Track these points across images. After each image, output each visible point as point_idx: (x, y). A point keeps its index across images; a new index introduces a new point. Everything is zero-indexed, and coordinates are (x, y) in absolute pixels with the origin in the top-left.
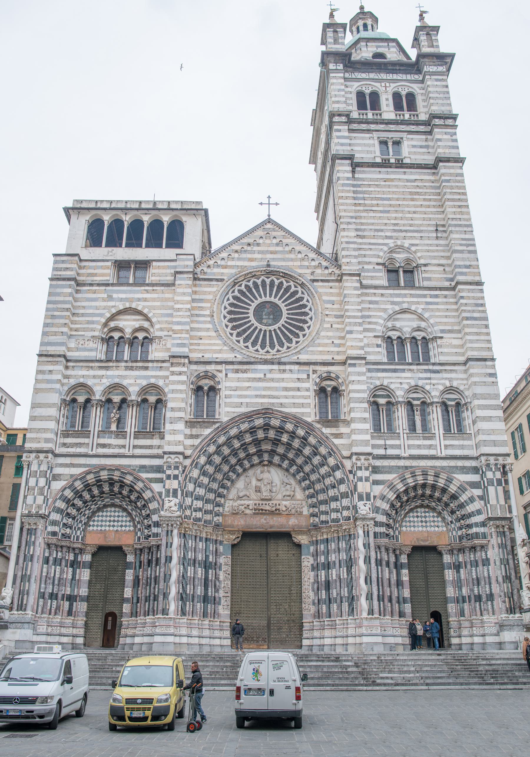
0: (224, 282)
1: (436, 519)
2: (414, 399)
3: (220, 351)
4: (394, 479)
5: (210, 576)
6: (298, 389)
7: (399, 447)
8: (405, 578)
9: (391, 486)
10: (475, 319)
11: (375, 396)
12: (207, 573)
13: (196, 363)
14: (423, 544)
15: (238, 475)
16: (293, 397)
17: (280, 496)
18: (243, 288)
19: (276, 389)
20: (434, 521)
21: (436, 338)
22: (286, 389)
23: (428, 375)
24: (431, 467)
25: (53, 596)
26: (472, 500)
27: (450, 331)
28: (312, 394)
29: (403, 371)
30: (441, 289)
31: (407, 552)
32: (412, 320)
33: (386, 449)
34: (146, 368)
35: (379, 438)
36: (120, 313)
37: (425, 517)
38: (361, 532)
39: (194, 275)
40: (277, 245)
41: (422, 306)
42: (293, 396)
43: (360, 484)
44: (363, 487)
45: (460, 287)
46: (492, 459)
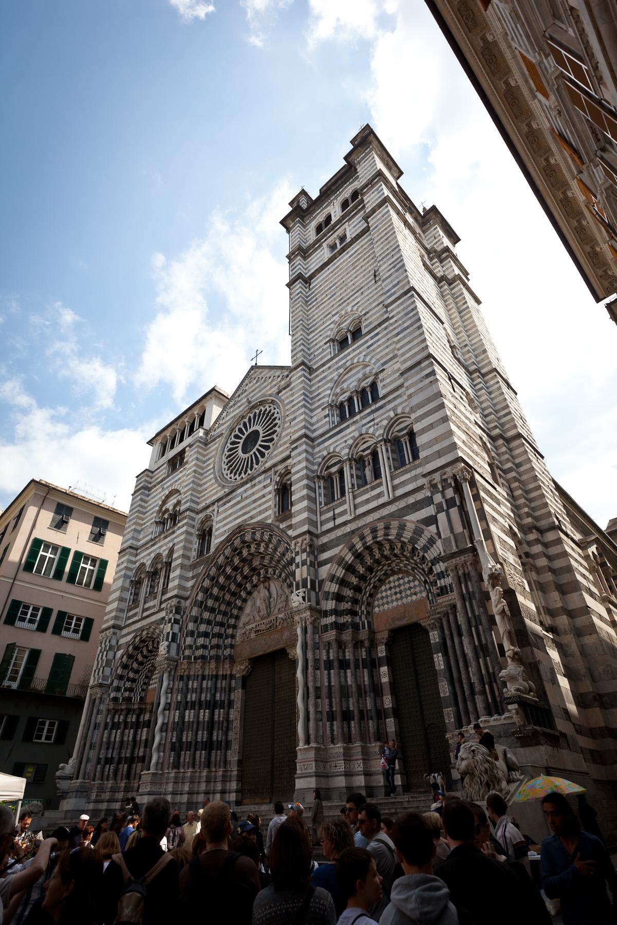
0: (224, 436)
1: (412, 584)
2: (364, 451)
3: (216, 493)
4: (341, 551)
5: (216, 717)
6: (264, 496)
7: (344, 513)
8: (385, 680)
9: (340, 561)
10: (407, 328)
11: (328, 468)
12: (212, 714)
13: (201, 511)
14: (399, 623)
15: (245, 601)
16: (260, 505)
17: (276, 610)
18: (237, 432)
19: (248, 505)
20: (410, 588)
21: (377, 374)
22: (255, 501)
23: (371, 417)
24: (379, 519)
25: (108, 761)
26: (432, 541)
27: (391, 359)
28: (273, 493)
29: (348, 427)
30: (379, 325)
31: (384, 641)
32: (358, 372)
33: (334, 519)
34: (173, 532)
35: (328, 511)
36: (168, 497)
37: (399, 585)
38: (299, 631)
39: (200, 442)
40: (257, 382)
41: (364, 353)
42: (256, 504)
43: (298, 571)
44: (301, 573)
45: (389, 309)
46: (437, 477)
